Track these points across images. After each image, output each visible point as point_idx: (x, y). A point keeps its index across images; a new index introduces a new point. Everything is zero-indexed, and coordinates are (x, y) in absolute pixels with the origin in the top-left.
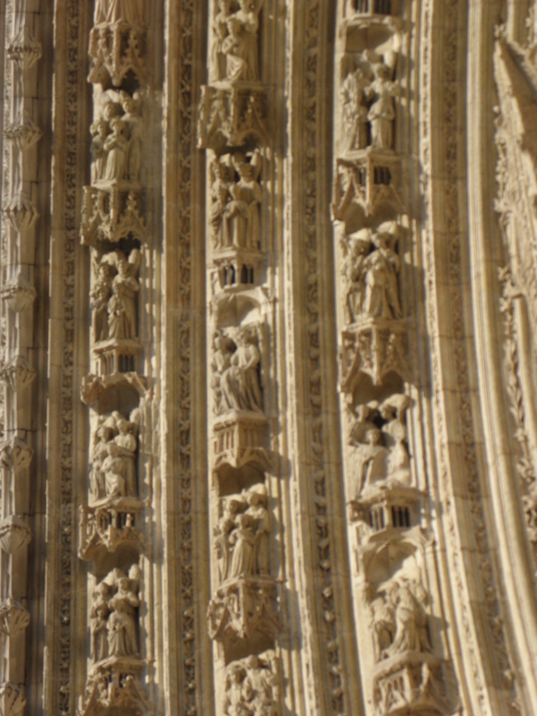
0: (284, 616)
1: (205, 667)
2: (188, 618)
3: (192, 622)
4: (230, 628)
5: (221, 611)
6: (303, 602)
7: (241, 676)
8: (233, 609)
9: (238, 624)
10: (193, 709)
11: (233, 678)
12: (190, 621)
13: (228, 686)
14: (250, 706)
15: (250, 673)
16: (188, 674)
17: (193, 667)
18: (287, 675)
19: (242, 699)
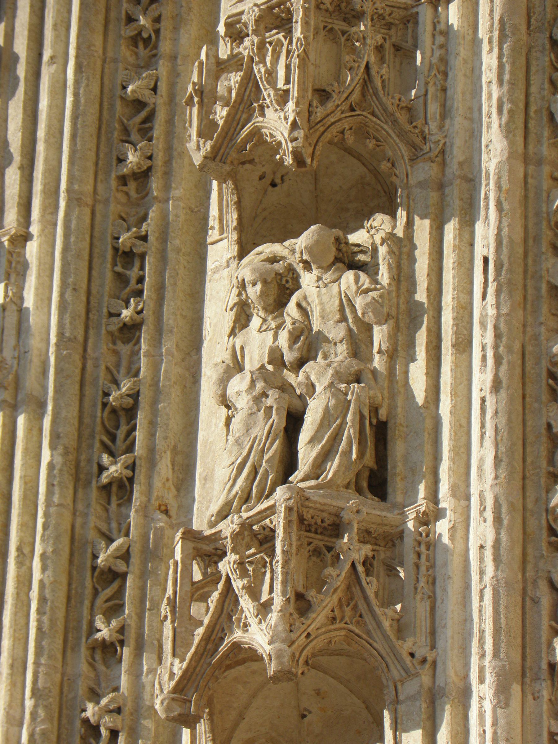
0: (433, 108)
1: (178, 264)
2: (138, 104)
3: (150, 118)
4: (257, 133)
5: (234, 79)
6: (489, 61)
7: (281, 288)
8: (271, 75)
9: (277, 123)
10: (126, 386)
11: (254, 292)
12: (143, 114)
13: (242, 317)
14: (295, 380)
15: (307, 279)
16: (122, 279)
17: (142, 256)
18: (421, 296)
19: (276, 357)
